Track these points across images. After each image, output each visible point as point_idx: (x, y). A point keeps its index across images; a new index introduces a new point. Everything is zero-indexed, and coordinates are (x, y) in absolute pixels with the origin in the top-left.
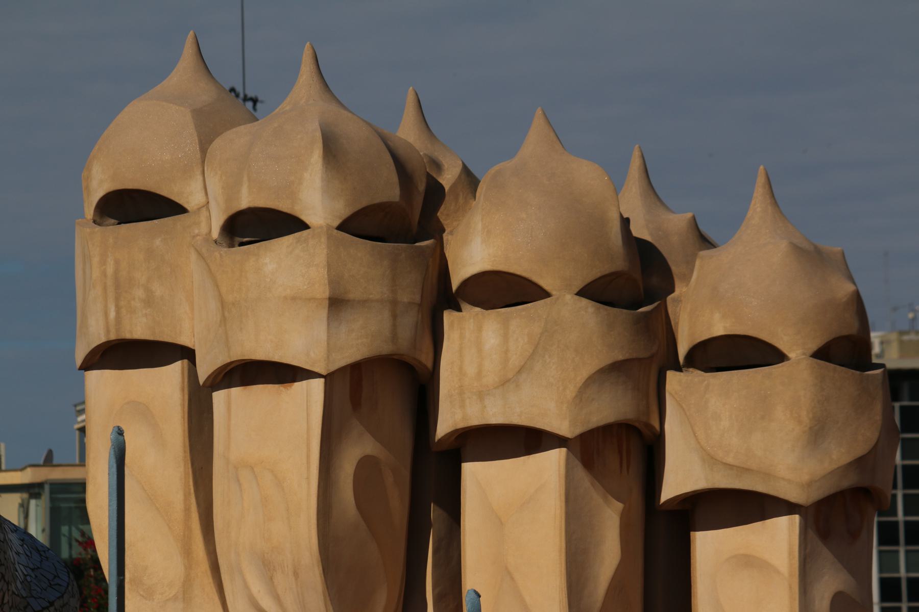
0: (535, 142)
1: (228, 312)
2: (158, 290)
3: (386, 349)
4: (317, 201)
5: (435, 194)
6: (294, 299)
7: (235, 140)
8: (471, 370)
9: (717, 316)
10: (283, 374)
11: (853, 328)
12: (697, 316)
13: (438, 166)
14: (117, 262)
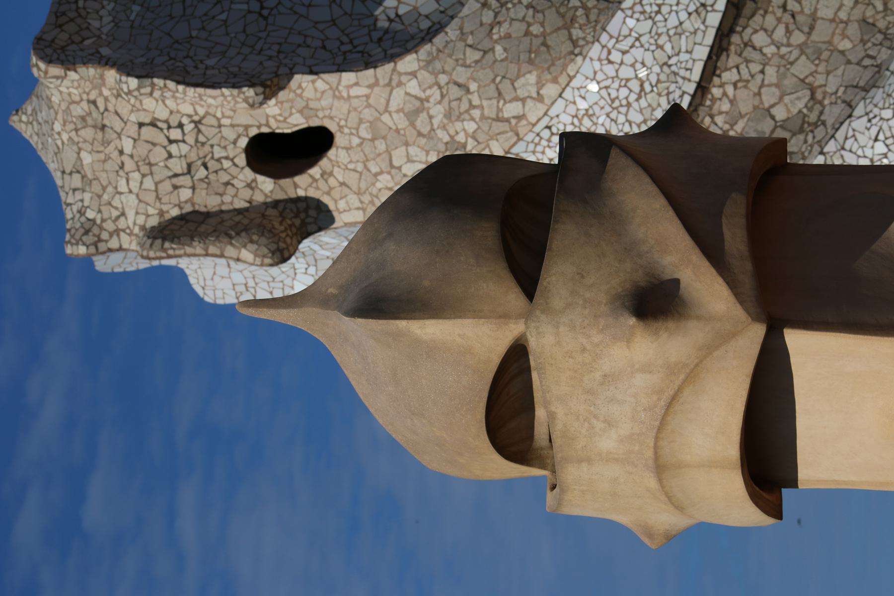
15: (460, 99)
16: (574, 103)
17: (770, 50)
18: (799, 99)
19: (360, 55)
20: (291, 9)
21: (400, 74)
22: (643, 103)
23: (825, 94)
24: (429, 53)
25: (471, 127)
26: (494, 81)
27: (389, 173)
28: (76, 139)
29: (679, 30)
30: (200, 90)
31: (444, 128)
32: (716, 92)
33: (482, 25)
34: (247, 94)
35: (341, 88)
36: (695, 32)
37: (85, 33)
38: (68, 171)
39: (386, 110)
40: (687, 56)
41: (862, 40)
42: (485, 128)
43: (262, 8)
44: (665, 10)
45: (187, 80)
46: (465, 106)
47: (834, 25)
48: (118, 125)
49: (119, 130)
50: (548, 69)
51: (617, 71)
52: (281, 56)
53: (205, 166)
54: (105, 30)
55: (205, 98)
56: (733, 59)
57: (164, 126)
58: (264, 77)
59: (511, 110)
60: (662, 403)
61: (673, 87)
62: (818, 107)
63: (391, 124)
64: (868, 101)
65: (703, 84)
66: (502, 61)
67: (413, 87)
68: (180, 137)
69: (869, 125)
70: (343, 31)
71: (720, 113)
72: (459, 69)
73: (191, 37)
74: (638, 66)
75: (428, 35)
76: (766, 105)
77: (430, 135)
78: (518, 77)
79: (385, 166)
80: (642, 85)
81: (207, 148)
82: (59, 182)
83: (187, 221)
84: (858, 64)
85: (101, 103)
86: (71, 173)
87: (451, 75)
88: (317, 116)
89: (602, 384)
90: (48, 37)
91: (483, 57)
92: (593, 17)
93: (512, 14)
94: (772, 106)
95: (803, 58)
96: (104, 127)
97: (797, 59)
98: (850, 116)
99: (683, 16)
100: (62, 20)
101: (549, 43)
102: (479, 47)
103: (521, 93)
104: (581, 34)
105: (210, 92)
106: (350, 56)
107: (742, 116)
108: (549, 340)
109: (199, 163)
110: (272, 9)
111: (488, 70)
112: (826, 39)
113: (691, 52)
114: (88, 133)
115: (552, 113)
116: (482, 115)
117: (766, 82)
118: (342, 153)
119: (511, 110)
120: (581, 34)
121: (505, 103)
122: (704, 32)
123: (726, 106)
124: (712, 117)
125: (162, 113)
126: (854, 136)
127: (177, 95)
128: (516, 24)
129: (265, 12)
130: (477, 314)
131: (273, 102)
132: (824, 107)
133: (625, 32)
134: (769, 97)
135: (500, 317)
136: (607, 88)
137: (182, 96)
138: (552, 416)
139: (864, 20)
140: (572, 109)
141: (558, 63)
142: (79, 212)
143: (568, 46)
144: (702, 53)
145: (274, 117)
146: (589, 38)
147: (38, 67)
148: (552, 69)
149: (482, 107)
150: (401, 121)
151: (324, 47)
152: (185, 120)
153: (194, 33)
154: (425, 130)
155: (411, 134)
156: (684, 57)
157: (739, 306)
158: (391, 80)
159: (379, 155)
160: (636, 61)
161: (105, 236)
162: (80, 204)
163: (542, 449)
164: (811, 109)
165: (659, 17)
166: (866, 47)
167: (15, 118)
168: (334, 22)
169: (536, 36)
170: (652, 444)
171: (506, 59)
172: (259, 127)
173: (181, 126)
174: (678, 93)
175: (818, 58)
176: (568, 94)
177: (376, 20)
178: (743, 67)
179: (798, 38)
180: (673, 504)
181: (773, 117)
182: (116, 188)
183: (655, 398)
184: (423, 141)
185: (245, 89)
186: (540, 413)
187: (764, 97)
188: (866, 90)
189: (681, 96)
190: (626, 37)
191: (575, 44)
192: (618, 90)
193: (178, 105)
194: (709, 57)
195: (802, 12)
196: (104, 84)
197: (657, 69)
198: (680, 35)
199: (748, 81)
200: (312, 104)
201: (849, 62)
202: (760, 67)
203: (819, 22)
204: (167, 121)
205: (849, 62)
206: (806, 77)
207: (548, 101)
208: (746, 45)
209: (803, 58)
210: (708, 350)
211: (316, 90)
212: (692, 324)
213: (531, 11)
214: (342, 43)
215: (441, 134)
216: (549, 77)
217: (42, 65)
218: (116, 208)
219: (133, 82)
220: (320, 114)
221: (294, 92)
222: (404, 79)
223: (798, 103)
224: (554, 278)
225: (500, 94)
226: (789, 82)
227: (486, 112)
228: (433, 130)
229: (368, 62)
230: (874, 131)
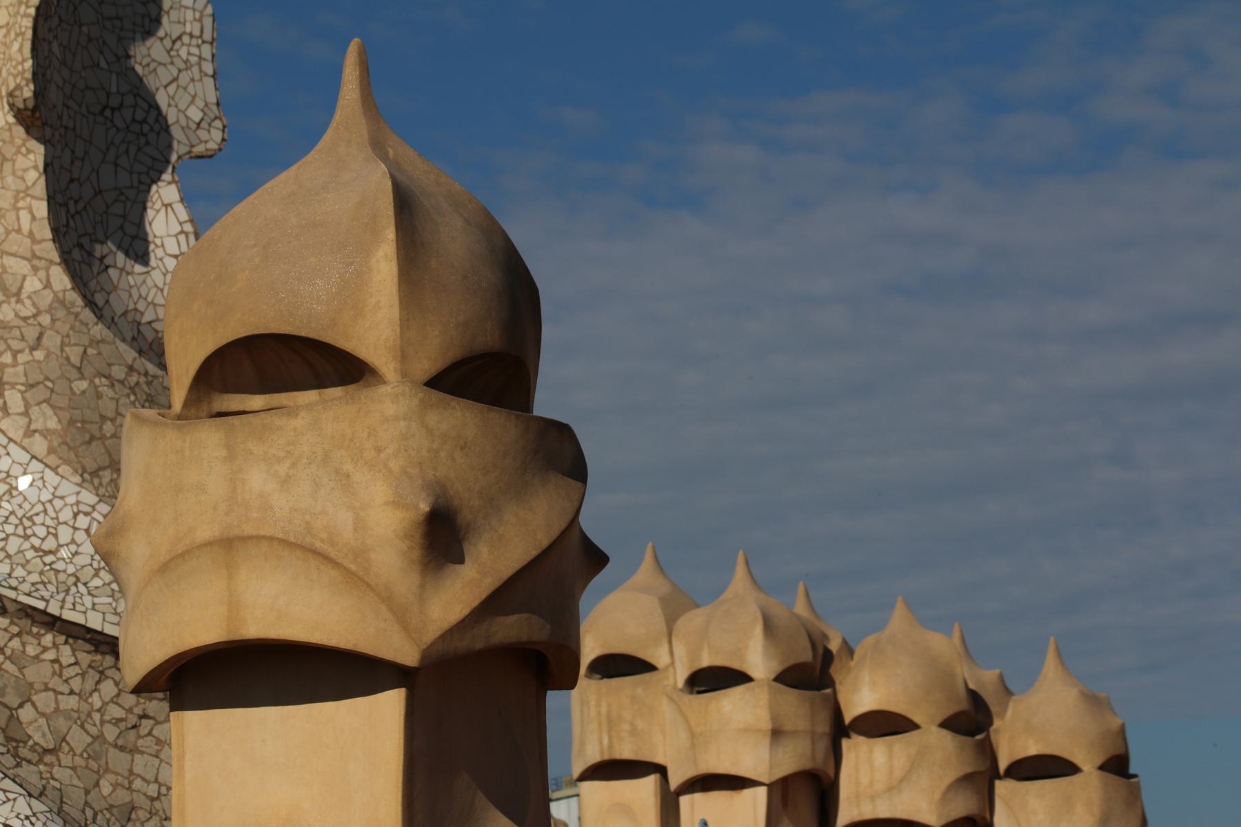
0: (899, 619)
1: (695, 739)
2: (640, 724)
3: (808, 765)
4: (759, 661)
5: (828, 657)
6: (746, 730)
7: (691, 621)
8: (865, 780)
9: (1031, 742)
10: (735, 783)
11: (1120, 751)
12: (1012, 743)
13: (825, 637)
14: (609, 705)
15: (23, 339)
16: (25, 473)
17: (96, 701)
18: (44, 735)
20: (112, 143)
21: (47, 270)
22: (30, 554)
23: (51, 765)
24: (73, 304)
26: (47, 379)
30: (29, 34)
32: (48, 639)
33: (109, 365)
34: (26, 89)
35: (28, 199)
36: (116, 614)
40: (89, 605)
41: (112, 806)
43: (113, 110)
46: (16, 345)
47: (126, 774)
50: (65, 443)
51: (65, 523)
52: (62, 131)
55: (20, 39)
56: (85, 659)
58: (43, 108)
60: (318, 544)
61: (52, 588)
62: (35, 758)
64: (48, 815)
65: (58, 623)
66: (71, 389)
67: (33, 284)
69: (22, 817)
71: (24, 644)
72: (59, 338)
73: (80, 26)
74: (73, 548)
75: (90, 303)
76: (34, 698)
78: (53, 407)
80: (50, 552)
84: (86, 803)
87: (51, 329)
89: (337, 472)
91: (74, 366)
93: (123, 400)
94: (33, 704)
95: (89, 740)
97: (87, 732)
98: (30, 795)
101: (94, 444)
102: (85, 362)
103: (35, 411)
104: (106, 480)
105: (28, 46)
106: (63, 211)
107: (21, 669)
108: (390, 409)
110: (112, 121)
111: (59, 372)
112: (110, 766)
115: (12, 448)
116: (7, 365)
117: (60, 697)
121: (22, 392)
123: (31, 650)
124: (19, 635)
126: (9, 800)
127: (23, 7)
128: (112, 405)
129: (108, 113)
130: (405, 323)
131: (11, 120)
134: (44, 700)
135: (403, 351)
136: (45, 511)
137: (22, 12)
138: (292, 412)
139: (133, 809)
140: (16, 470)
141: (72, 455)
143: (91, 466)
144: (94, 622)
146: (102, 491)
148: (65, 447)
151: (71, 181)
153: (85, 29)
157: (439, 633)
158: (40, 258)
160: (78, 546)
163: (210, 403)
168: (99, 192)
169: (101, 428)
170: (262, 533)
171: (74, 394)
174: (47, 595)
176: (36, 465)
177: (102, 243)
178: (77, 669)
179: (111, 733)
180: (172, 560)
181: (21, 706)
183: (324, 536)
185: (32, 87)
186: (257, 401)
187: (43, 694)
188: (60, 812)
189: (43, 598)
191: (95, 474)
192: (43, 524)
193: (7, 7)
194: (90, 630)
195: (140, 737)
197: (71, 569)
198: (112, 596)
199: (60, 676)
201: (87, 792)
202: (77, 690)
203: (129, 757)
205: (87, 792)
206: (68, 744)
207: (26, 442)
208: (101, 673)
209: (89, 740)
210: (387, 598)
211: (25, 170)
212: (415, 578)
214: (76, 202)
216: (55, 444)
221: (24, 145)
222: (42, 273)
223: (39, 735)
224: (459, 414)
225: (32, 386)
226: (61, 724)
227: (9, 370)
229: (59, 233)
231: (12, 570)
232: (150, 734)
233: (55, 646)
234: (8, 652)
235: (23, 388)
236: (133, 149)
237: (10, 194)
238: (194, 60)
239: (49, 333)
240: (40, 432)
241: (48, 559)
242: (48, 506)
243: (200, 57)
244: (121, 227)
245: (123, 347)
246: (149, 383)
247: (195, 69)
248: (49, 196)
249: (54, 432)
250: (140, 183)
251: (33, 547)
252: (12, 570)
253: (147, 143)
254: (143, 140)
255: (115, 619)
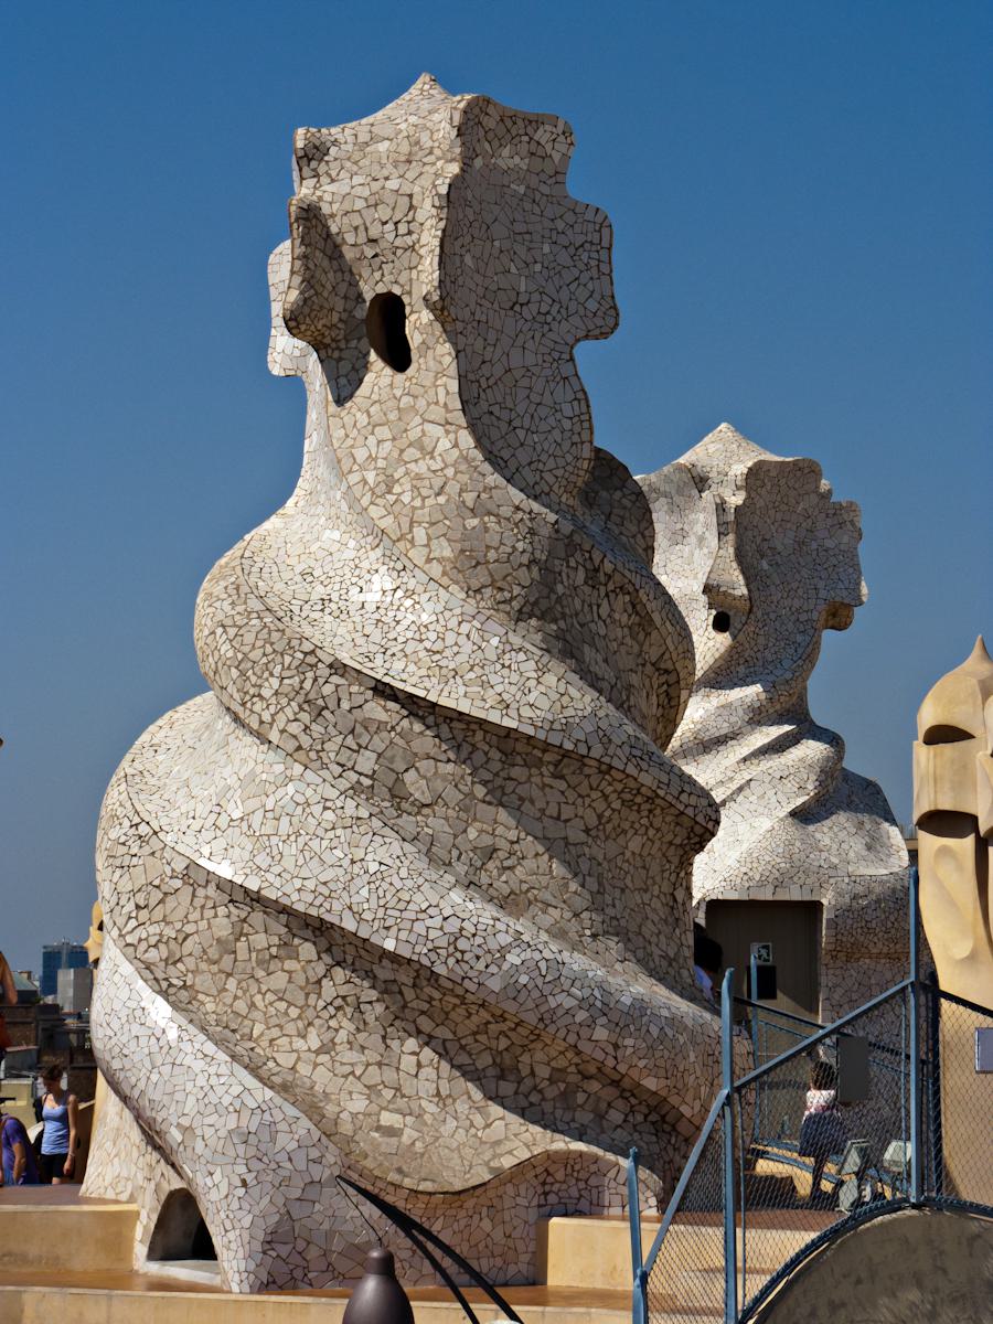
15: (431, 488)
16: (425, 591)
18: (423, 793)
19: (476, 395)
20: (521, 331)
21: (456, 433)
22: (422, 654)
23: (427, 816)
24: (474, 460)
25: (406, 498)
27: (369, 424)
28: (400, 137)
29: (486, 685)
30: (437, 251)
31: (407, 474)
35: (444, 378)
37: (496, 143)
38: (373, 129)
39: (424, 420)
40: (462, 693)
42: (405, 511)
43: (522, 305)
44: (506, 671)
45: (447, 239)
46: (425, 492)
48: (411, 175)
49: (406, 176)
50: (455, 567)
53: (376, 255)
54: (500, 162)
57: (409, 218)
58: (452, 309)
59: (420, 534)
63: (412, 424)
64: (417, 855)
66: (464, 525)
67: (445, 444)
68: (400, 232)
69: (394, 856)
70: (500, 379)
71: (411, 723)
72: (458, 486)
73: (493, 241)
74: (455, 649)
77: (401, 461)
78: (448, 540)
79: (375, 419)
81: (391, 257)
82: (364, 121)
83: (326, 240)
84: (454, 845)
85: (431, 159)
86: (371, 132)
88: (420, 357)
90: (491, 110)
91: (468, 508)
92: (502, 606)
94: (417, 769)
95: (462, 797)
96: (410, 162)
98: (404, 840)
99: (499, 689)
100: (509, 123)
101: (479, 568)
103: (434, 543)
105: (436, 259)
109: (378, 251)
111: (456, 513)
113: (465, 696)
114: (405, 148)
117: (439, 764)
118: (388, 381)
119: (420, 534)
120: (486, 596)
122: (483, 708)
125: (421, 215)
129: (517, 308)
131: (432, 318)
132: (415, 815)
133: (486, 636)
139: (495, 850)
142: (336, 140)
143: (475, 584)
145: (419, 318)
147: (462, 101)
149: (423, 507)
150: (414, 434)
151: (484, 362)
152: (415, 237)
153: (497, 243)
154: (406, 456)
155: (403, 443)
156: (462, 689)
158: (450, 424)
159: (385, 414)
161: (314, 164)
162: (342, 141)
164: (413, 804)
165: (499, 666)
166: (469, 852)
167: (427, 79)
169: (485, 555)
171: (465, 529)
172: (410, 304)
173: (410, 233)
174: (429, 686)
175: (461, 809)
181: (406, 770)
182: (356, 174)
184: (396, 454)
190: (482, 637)
191: (478, 591)
194: (461, 713)
196: (447, 161)
198: (482, 686)
200: (430, 352)
201: (455, 836)
204: (414, 220)
205: (455, 836)
207: (426, 567)
209: (462, 797)
213: (510, 550)
214: (487, 379)
215: (401, 471)
216: (448, 568)
217: (462, 105)
218: (338, 175)
219: (444, 190)
220: (421, 361)
222: (452, 436)
225: (435, 524)
227: (420, 511)
228: (406, 463)
230: (389, 861)
231: (406, 666)
232: (513, 792)
233: (437, 725)
234: (398, 729)
235: (427, 525)
236: (538, 336)
237: (432, 374)
238: (594, 263)
239: (451, 482)
240: (438, 560)
241: (437, 657)
242: (440, 616)
243: (599, 261)
244: (528, 397)
245: (513, 491)
246: (531, 520)
247: (594, 271)
248: (459, 376)
249: (449, 559)
250: (544, 361)
251: (425, 648)
252: (406, 666)
253: (550, 330)
254: (546, 327)
255: (482, 704)
